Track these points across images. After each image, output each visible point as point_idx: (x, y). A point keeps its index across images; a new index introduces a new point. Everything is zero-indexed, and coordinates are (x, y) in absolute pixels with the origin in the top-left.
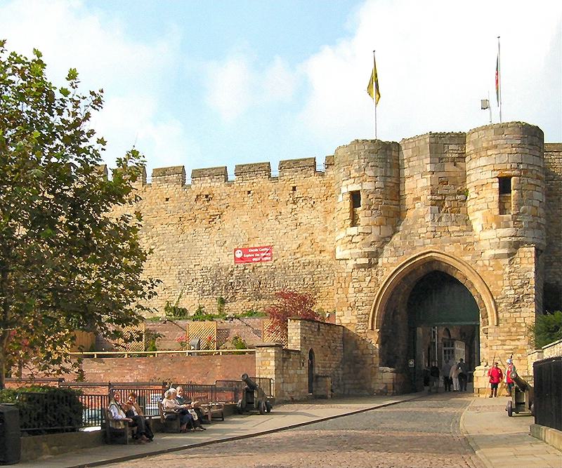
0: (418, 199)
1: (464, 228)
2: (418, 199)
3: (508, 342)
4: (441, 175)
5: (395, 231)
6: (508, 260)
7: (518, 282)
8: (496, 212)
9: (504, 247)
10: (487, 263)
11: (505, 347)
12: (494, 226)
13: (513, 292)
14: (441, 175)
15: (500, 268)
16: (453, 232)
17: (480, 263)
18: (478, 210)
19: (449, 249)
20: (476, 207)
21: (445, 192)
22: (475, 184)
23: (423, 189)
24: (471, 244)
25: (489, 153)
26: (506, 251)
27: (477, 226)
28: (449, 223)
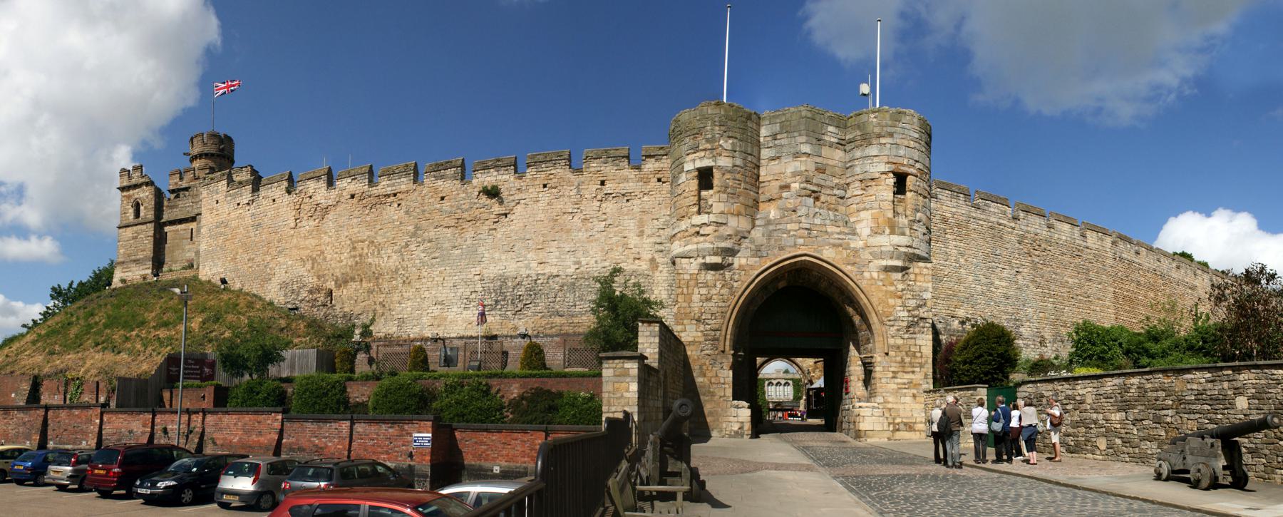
0: (786, 187)
1: (846, 231)
2: (786, 187)
3: (900, 375)
4: (819, 160)
5: (754, 226)
6: (899, 275)
7: (912, 303)
8: (890, 215)
9: (898, 258)
10: (875, 275)
11: (899, 381)
12: (888, 231)
13: (906, 314)
14: (819, 160)
15: (892, 284)
16: (832, 233)
17: (866, 275)
18: (865, 209)
19: (828, 254)
20: (862, 206)
21: (822, 183)
22: (861, 177)
23: (795, 174)
24: (856, 251)
25: (883, 141)
26: (899, 263)
27: (864, 229)
28: (828, 222)
